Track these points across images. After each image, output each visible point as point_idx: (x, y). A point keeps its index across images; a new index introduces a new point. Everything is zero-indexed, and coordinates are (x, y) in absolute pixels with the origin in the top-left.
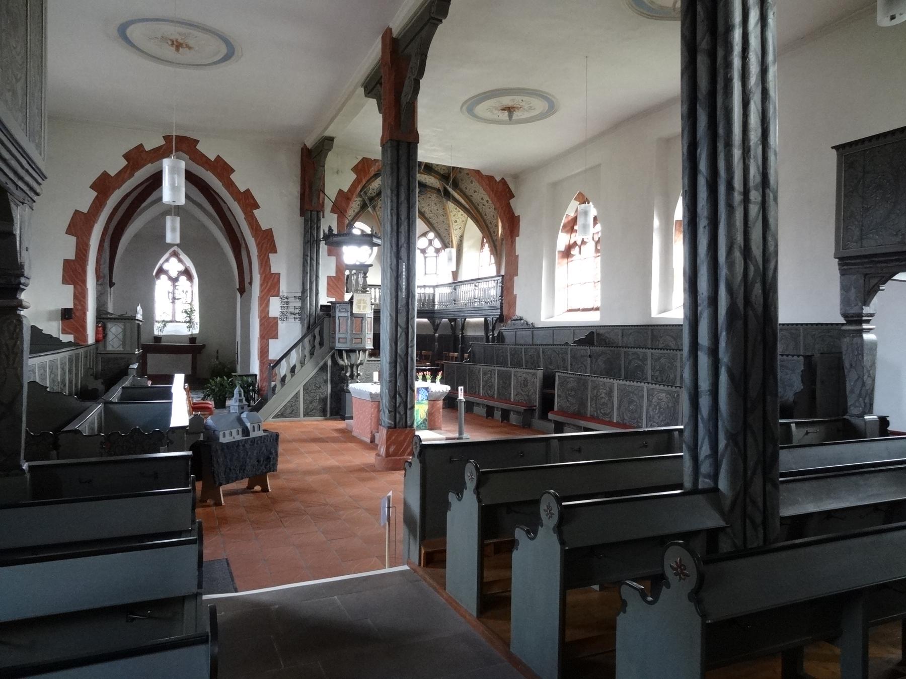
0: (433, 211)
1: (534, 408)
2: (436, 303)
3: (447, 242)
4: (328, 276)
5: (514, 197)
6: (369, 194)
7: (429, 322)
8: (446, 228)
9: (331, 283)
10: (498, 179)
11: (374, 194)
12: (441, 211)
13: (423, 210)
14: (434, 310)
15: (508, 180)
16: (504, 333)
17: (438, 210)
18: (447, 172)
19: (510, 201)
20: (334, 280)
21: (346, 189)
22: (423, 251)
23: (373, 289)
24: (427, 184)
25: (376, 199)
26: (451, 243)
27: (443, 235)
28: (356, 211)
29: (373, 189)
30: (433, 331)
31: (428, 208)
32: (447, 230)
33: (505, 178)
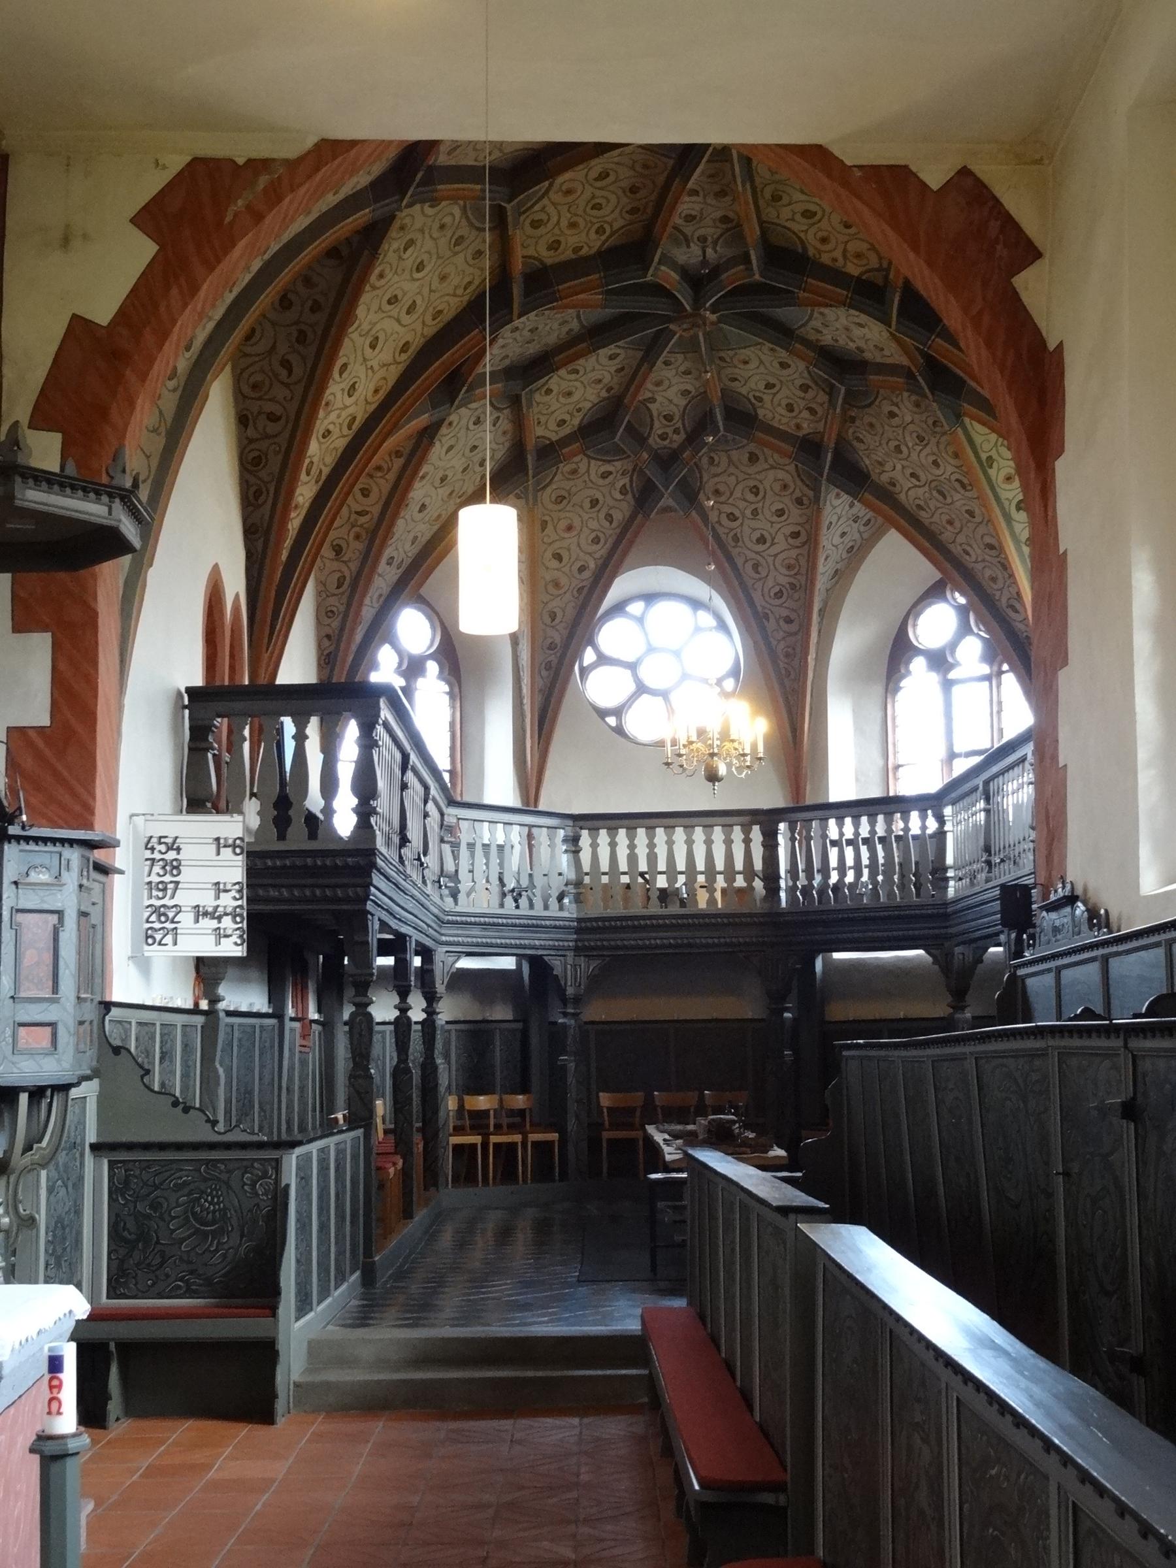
0: (923, 478)
1: (768, 1498)
2: (950, 874)
3: (1004, 601)
4: (10, 730)
5: (1038, 255)
6: (654, 441)
7: (930, 959)
8: (988, 540)
9: (28, 763)
10: (935, 177)
11: (679, 438)
12: (950, 469)
13: (885, 478)
14: (946, 904)
15: (990, 172)
16: (1030, 982)
17: (935, 463)
18: (874, 263)
19: (1019, 281)
20: (40, 744)
21: (103, 313)
22: (940, 661)
23: (699, 834)
24: (868, 356)
25: (686, 454)
26: (1018, 606)
27: (985, 574)
28: (618, 516)
29: (668, 418)
30: (950, 999)
31: (899, 467)
32: (991, 547)
33: (975, 168)
